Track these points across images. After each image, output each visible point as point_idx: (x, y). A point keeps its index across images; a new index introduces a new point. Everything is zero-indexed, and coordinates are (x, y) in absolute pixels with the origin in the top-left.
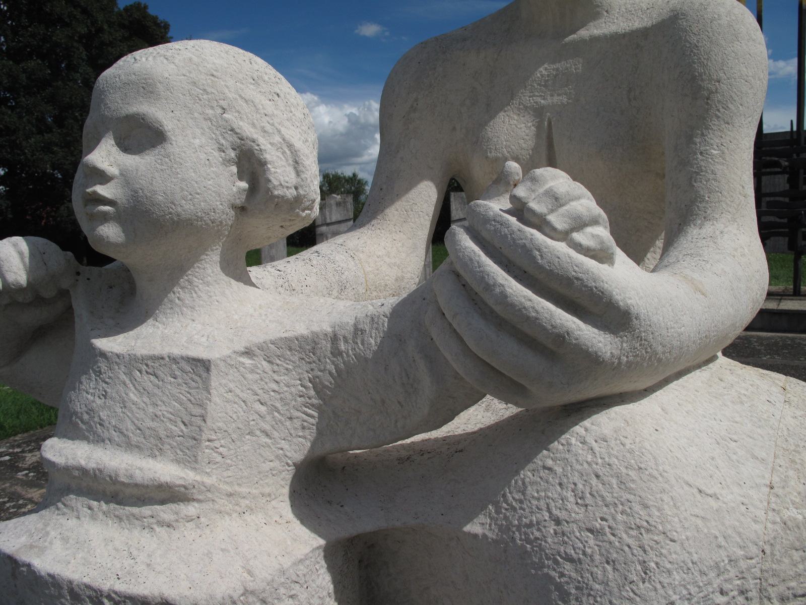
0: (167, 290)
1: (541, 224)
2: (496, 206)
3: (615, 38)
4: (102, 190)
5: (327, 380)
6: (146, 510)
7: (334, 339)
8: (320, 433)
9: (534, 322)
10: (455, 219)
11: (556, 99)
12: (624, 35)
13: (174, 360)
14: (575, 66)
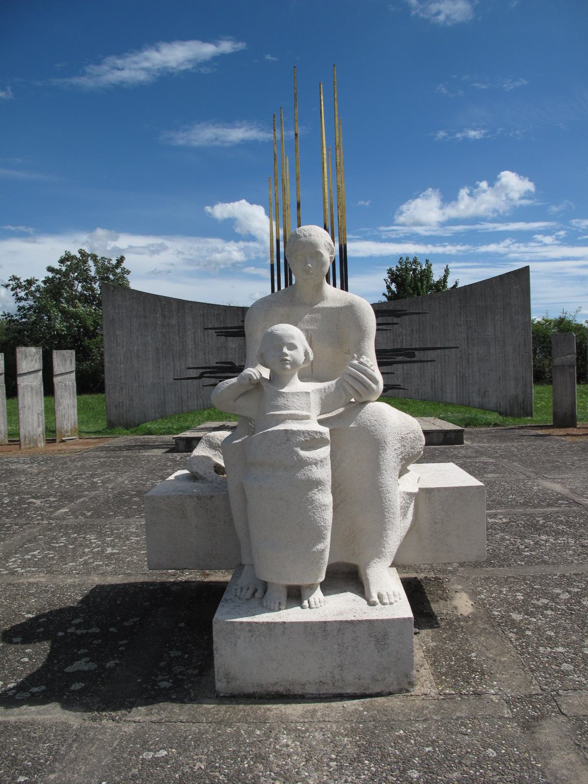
0: (290, 379)
1: (366, 366)
2: (356, 362)
3: (331, 309)
4: (288, 358)
5: (324, 398)
6: (304, 421)
7: (325, 389)
8: (321, 409)
9: (366, 382)
10: (58, 373)
11: (312, 327)
12: (334, 308)
13: (302, 392)
14: (318, 316)
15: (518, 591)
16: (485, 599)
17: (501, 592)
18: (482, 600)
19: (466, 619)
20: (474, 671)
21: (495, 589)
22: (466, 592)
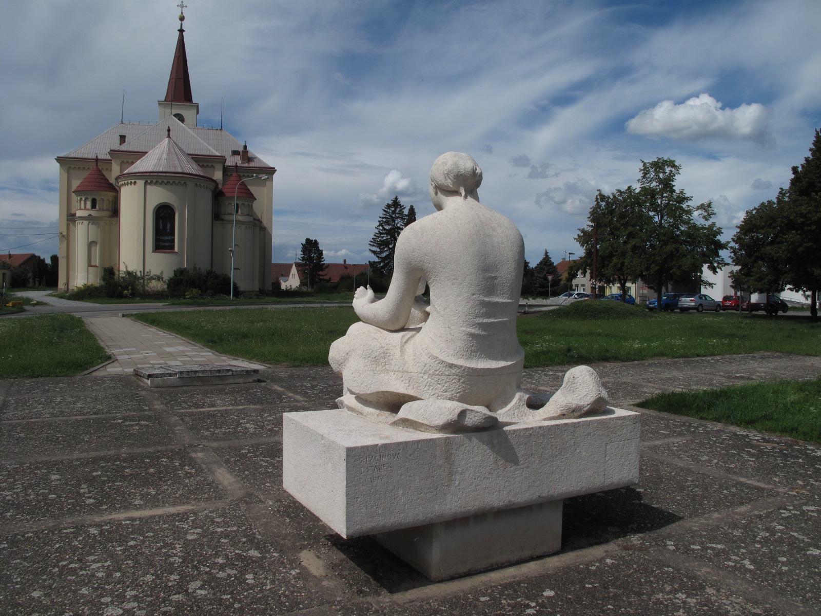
15: (252, 587)
16: (290, 569)
17: (272, 582)
18: (293, 568)
19: (303, 548)
20: (285, 511)
21: (281, 587)
22: (315, 577)
